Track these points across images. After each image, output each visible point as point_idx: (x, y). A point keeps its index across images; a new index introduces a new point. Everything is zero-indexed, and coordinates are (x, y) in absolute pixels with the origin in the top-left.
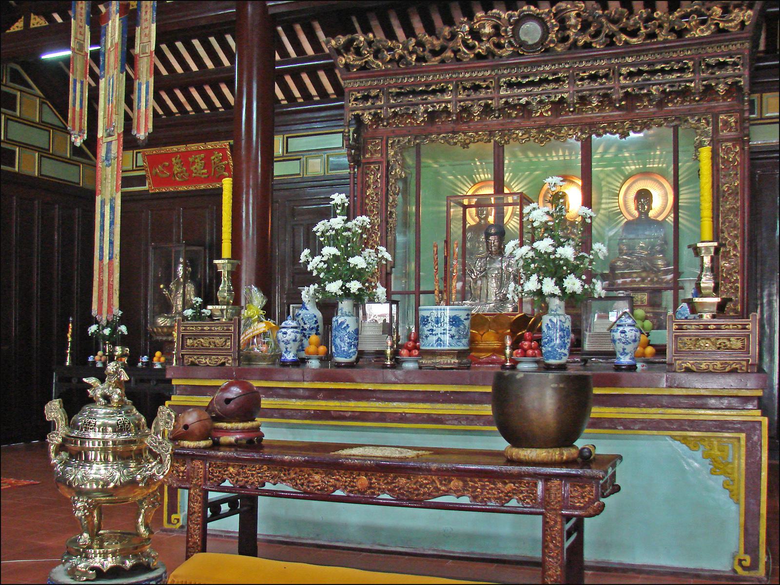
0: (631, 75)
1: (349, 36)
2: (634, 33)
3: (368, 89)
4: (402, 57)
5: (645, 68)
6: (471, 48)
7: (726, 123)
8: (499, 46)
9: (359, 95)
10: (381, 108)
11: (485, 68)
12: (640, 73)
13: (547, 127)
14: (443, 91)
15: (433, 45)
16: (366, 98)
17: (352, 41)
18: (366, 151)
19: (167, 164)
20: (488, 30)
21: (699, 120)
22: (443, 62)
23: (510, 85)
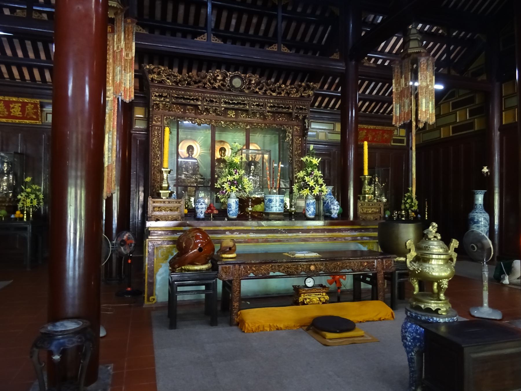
0: (271, 107)
2: (274, 91)
3: (162, 93)
4: (180, 81)
5: (276, 105)
7: (296, 129)
11: (217, 94)
12: (274, 106)
13: (234, 121)
14: (197, 100)
16: (160, 96)
21: (288, 127)
23: (226, 103)
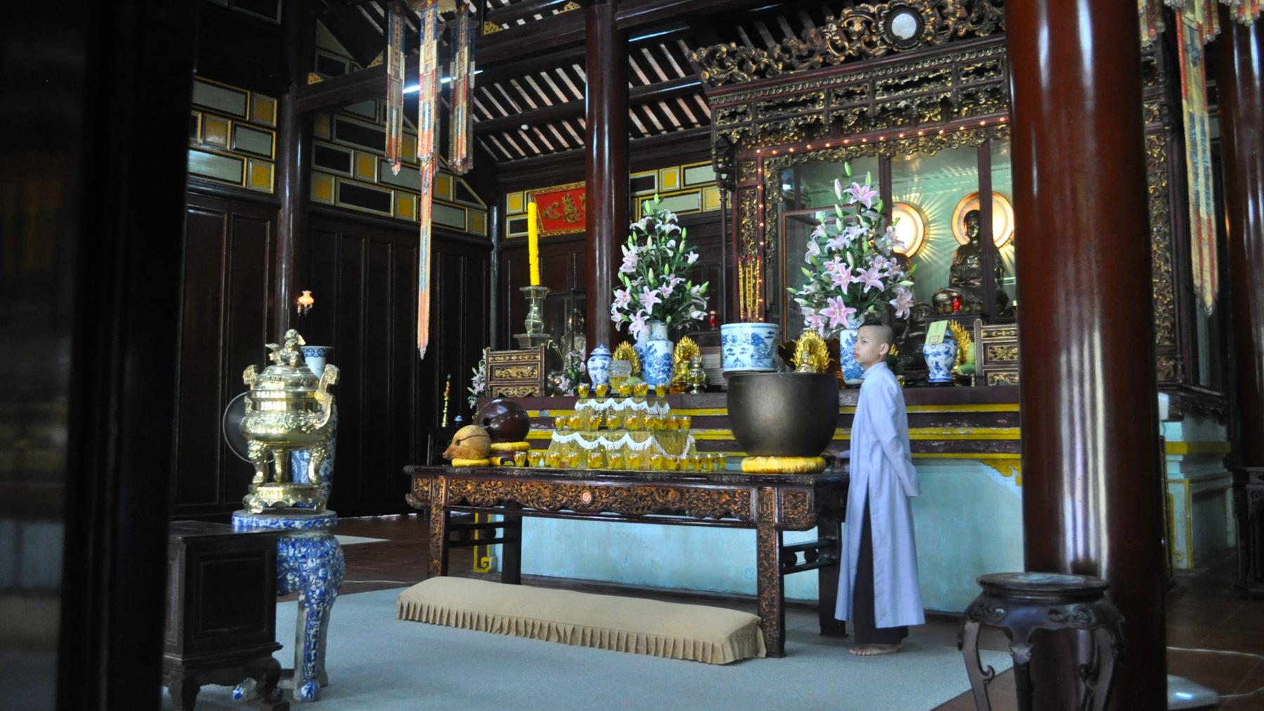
1: (711, 48)
6: (841, 49)
8: (871, 44)
9: (726, 113)
10: (748, 124)
14: (814, 101)
15: (799, 50)
16: (733, 115)
17: (715, 52)
18: (741, 175)
19: (557, 204)
20: (857, 27)
22: (812, 67)
23: (887, 88)
